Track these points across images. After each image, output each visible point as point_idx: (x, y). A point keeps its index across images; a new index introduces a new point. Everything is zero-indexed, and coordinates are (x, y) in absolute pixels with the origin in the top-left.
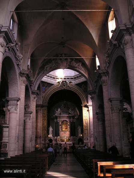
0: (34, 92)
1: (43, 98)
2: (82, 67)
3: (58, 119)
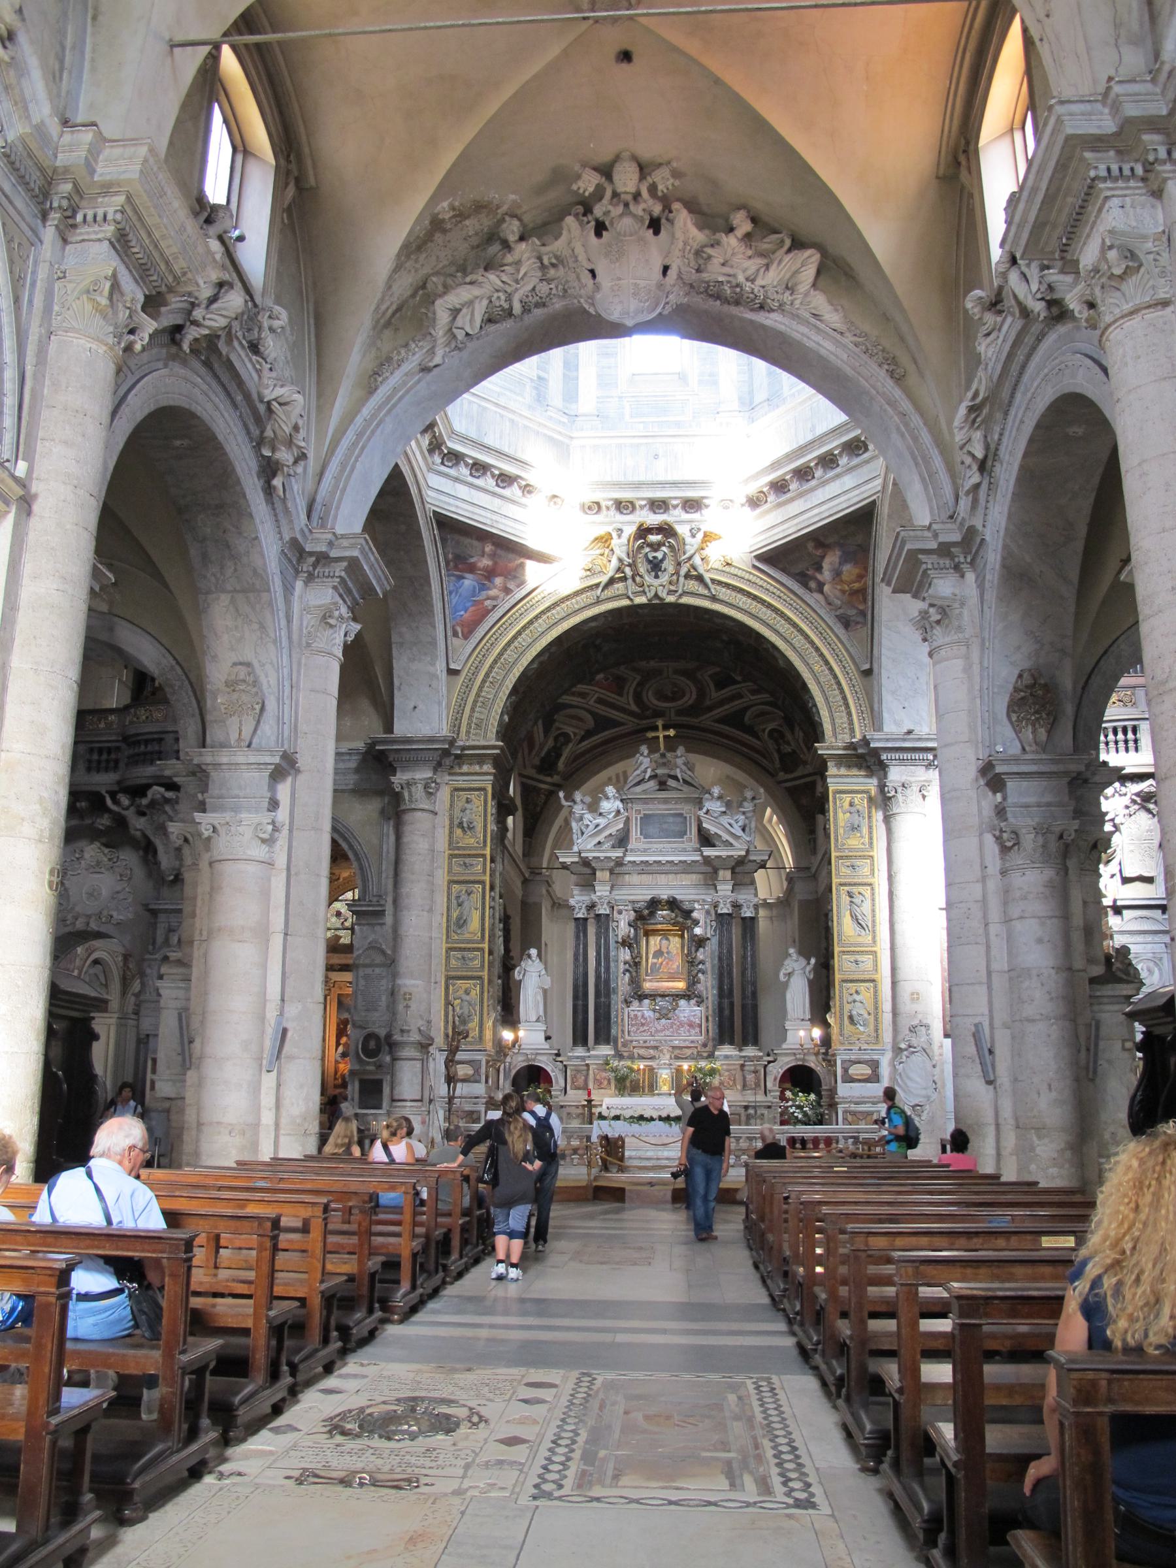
0: (323, 548)
1: (461, 678)
2: (819, 301)
3: (602, 890)
